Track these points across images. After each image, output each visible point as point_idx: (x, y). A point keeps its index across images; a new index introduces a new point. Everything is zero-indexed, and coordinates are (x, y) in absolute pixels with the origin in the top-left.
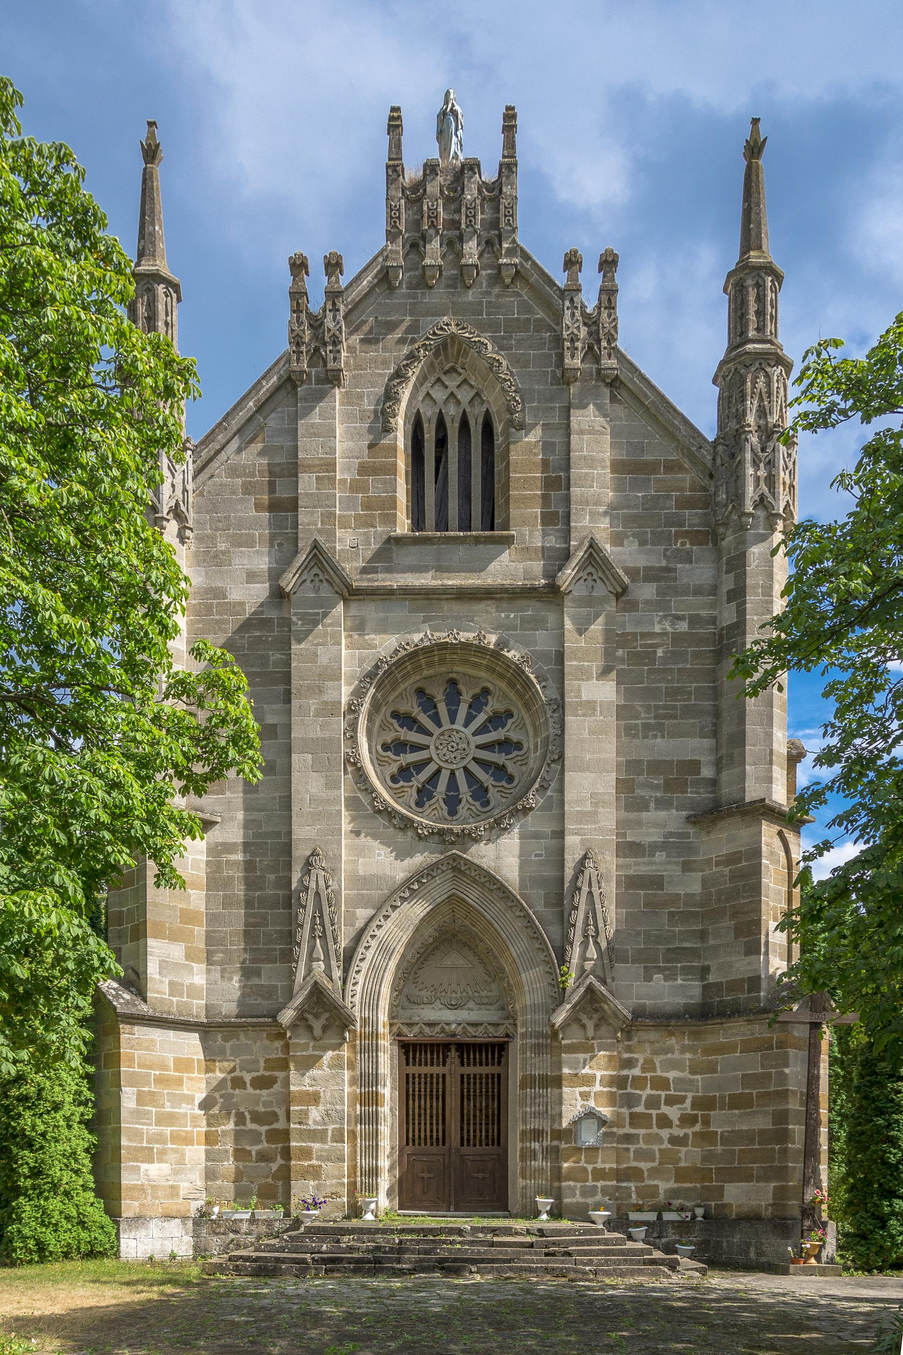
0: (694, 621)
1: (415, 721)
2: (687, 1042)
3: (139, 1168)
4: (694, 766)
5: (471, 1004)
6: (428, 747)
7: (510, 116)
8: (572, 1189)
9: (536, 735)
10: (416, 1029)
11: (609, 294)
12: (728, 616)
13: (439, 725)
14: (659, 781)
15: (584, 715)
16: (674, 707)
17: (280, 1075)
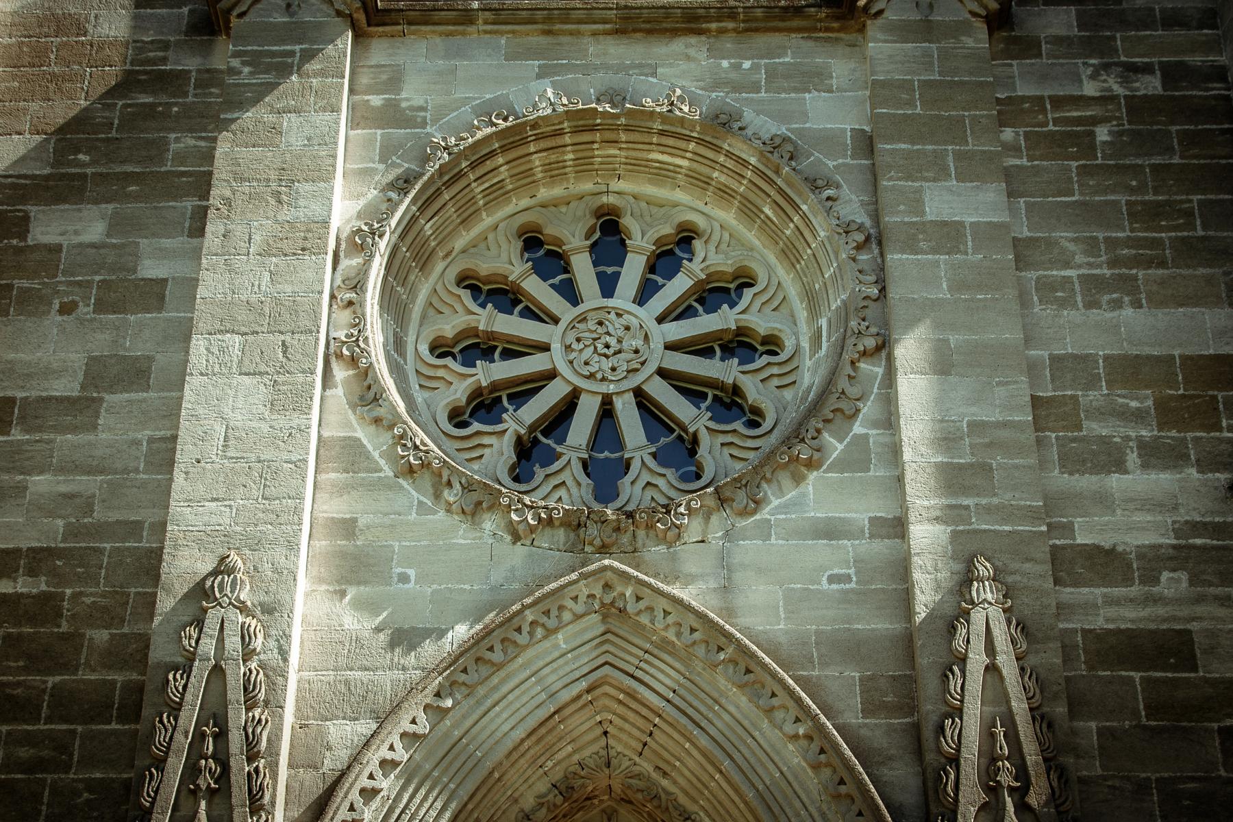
0: (1172, 74)
6: (545, 348)
9: (814, 310)
13: (574, 299)
14: (1143, 400)
15: (934, 251)
16: (1155, 243)
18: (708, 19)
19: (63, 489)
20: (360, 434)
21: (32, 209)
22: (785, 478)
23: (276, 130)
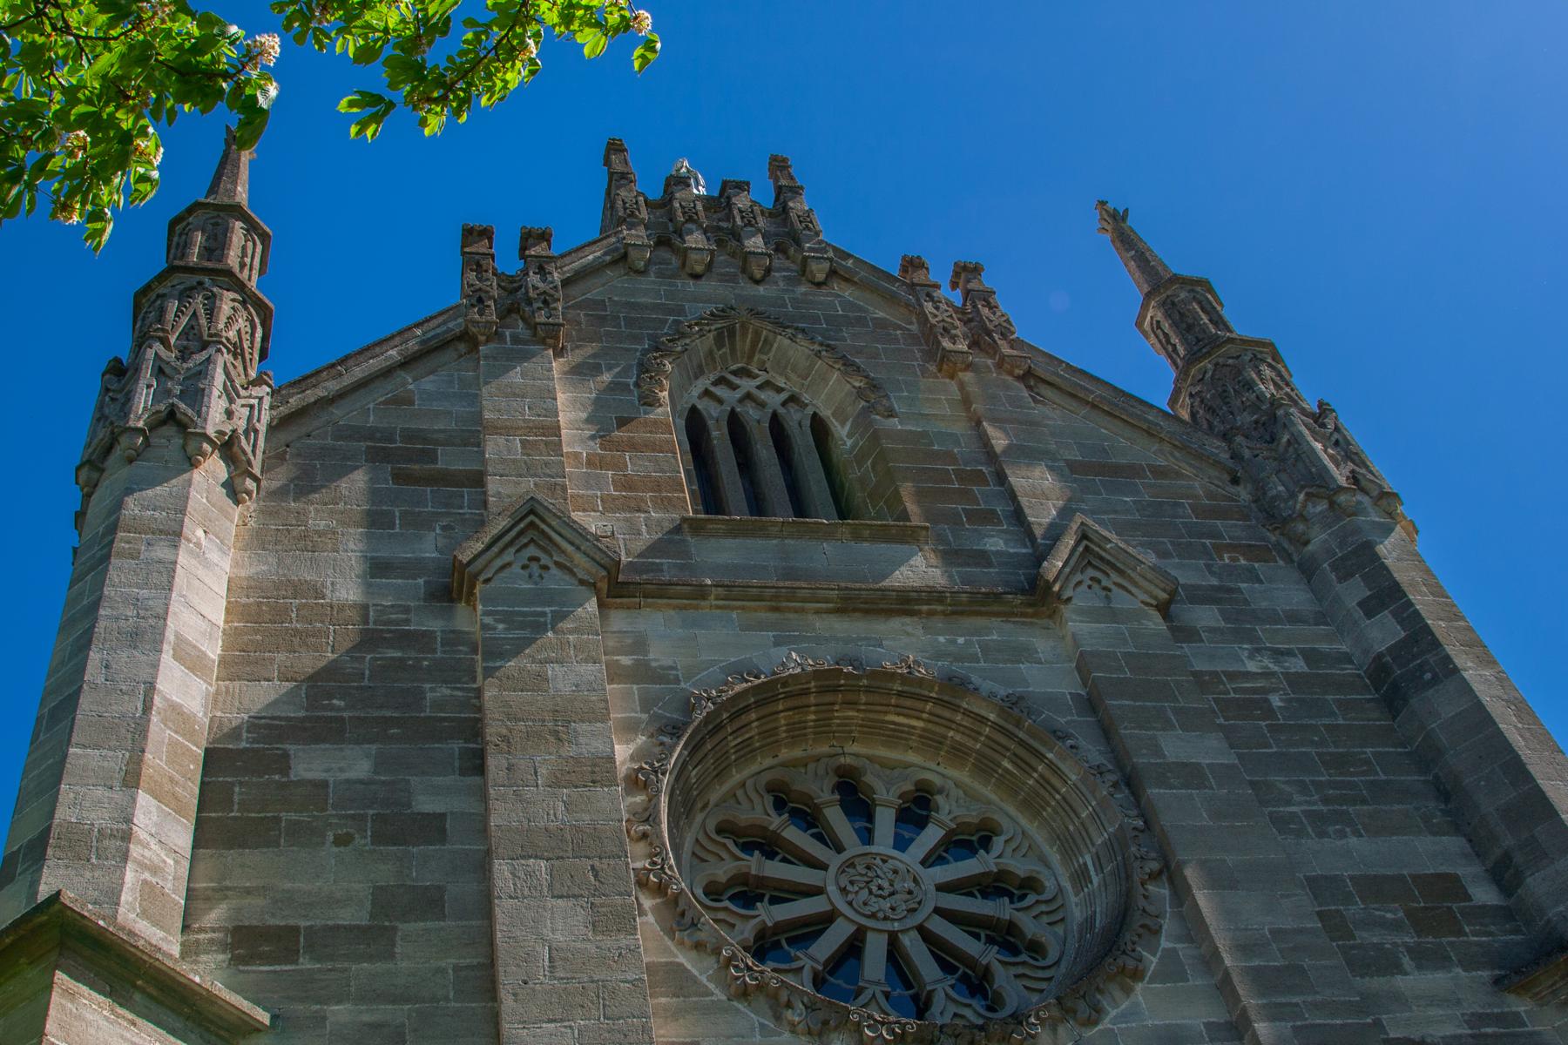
0: (1311, 656)
18: (919, 601)
19: (366, 1018)
20: (681, 959)
21: (291, 748)
23: (542, 677)
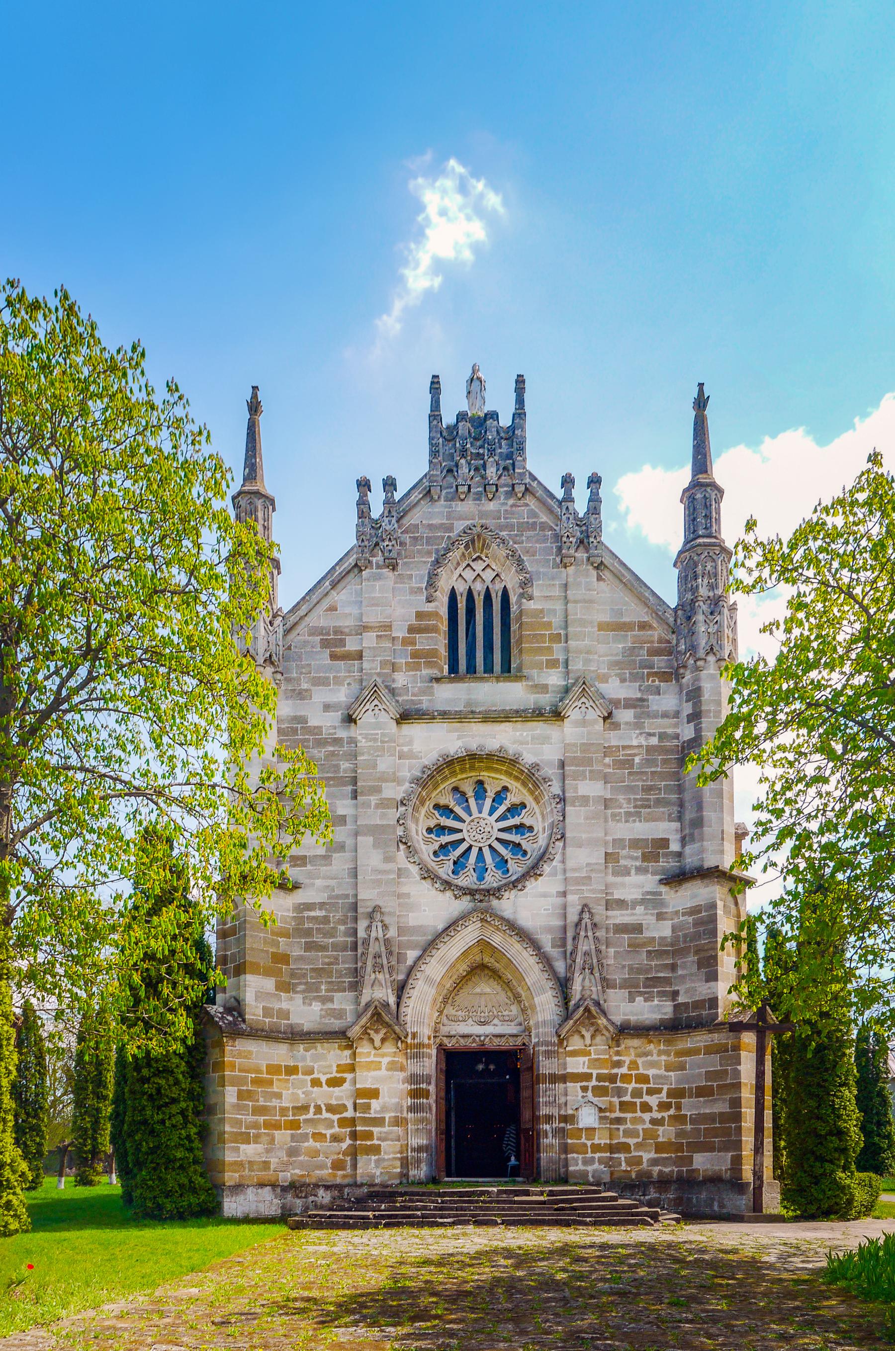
1: (452, 811)
2: (662, 1047)
3: (238, 1148)
4: (665, 843)
5: (496, 1021)
7: (520, 381)
8: (576, 1160)
10: (454, 1040)
11: (595, 502)
12: (687, 732)
14: (638, 853)
16: (648, 800)
17: (349, 1076)
22: (532, 879)
